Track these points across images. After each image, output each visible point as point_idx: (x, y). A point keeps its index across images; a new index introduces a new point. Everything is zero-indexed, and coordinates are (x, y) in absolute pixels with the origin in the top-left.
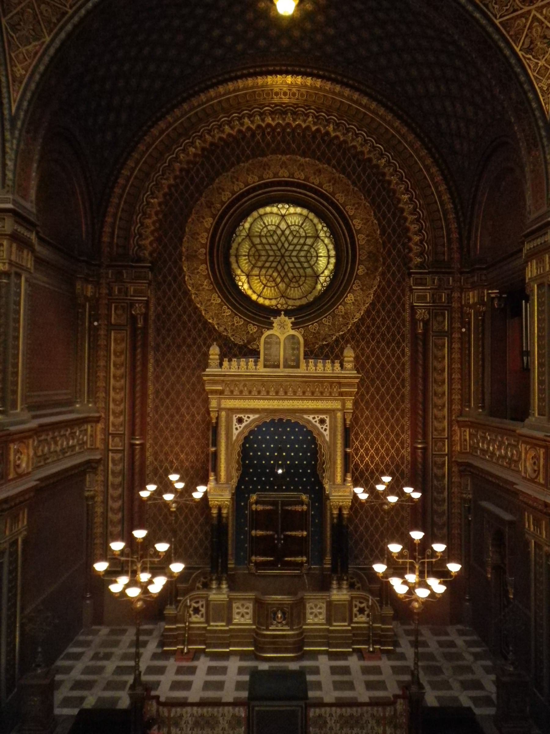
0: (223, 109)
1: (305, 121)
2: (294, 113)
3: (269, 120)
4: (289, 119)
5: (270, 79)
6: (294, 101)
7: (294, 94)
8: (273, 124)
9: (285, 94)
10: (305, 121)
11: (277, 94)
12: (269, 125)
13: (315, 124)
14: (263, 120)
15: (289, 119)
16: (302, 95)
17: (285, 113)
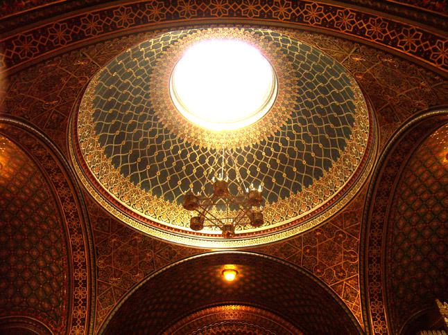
0: (198, 324)
1: (242, 328)
2: (236, 325)
3: (223, 329)
4: (234, 327)
5: (223, 308)
6: (236, 318)
7: (236, 315)
8: (226, 331)
9: (231, 315)
10: (242, 328)
11: (227, 315)
12: (223, 332)
13: (248, 330)
14: (220, 329)
15: (234, 327)
16: (240, 315)
17: (232, 325)
